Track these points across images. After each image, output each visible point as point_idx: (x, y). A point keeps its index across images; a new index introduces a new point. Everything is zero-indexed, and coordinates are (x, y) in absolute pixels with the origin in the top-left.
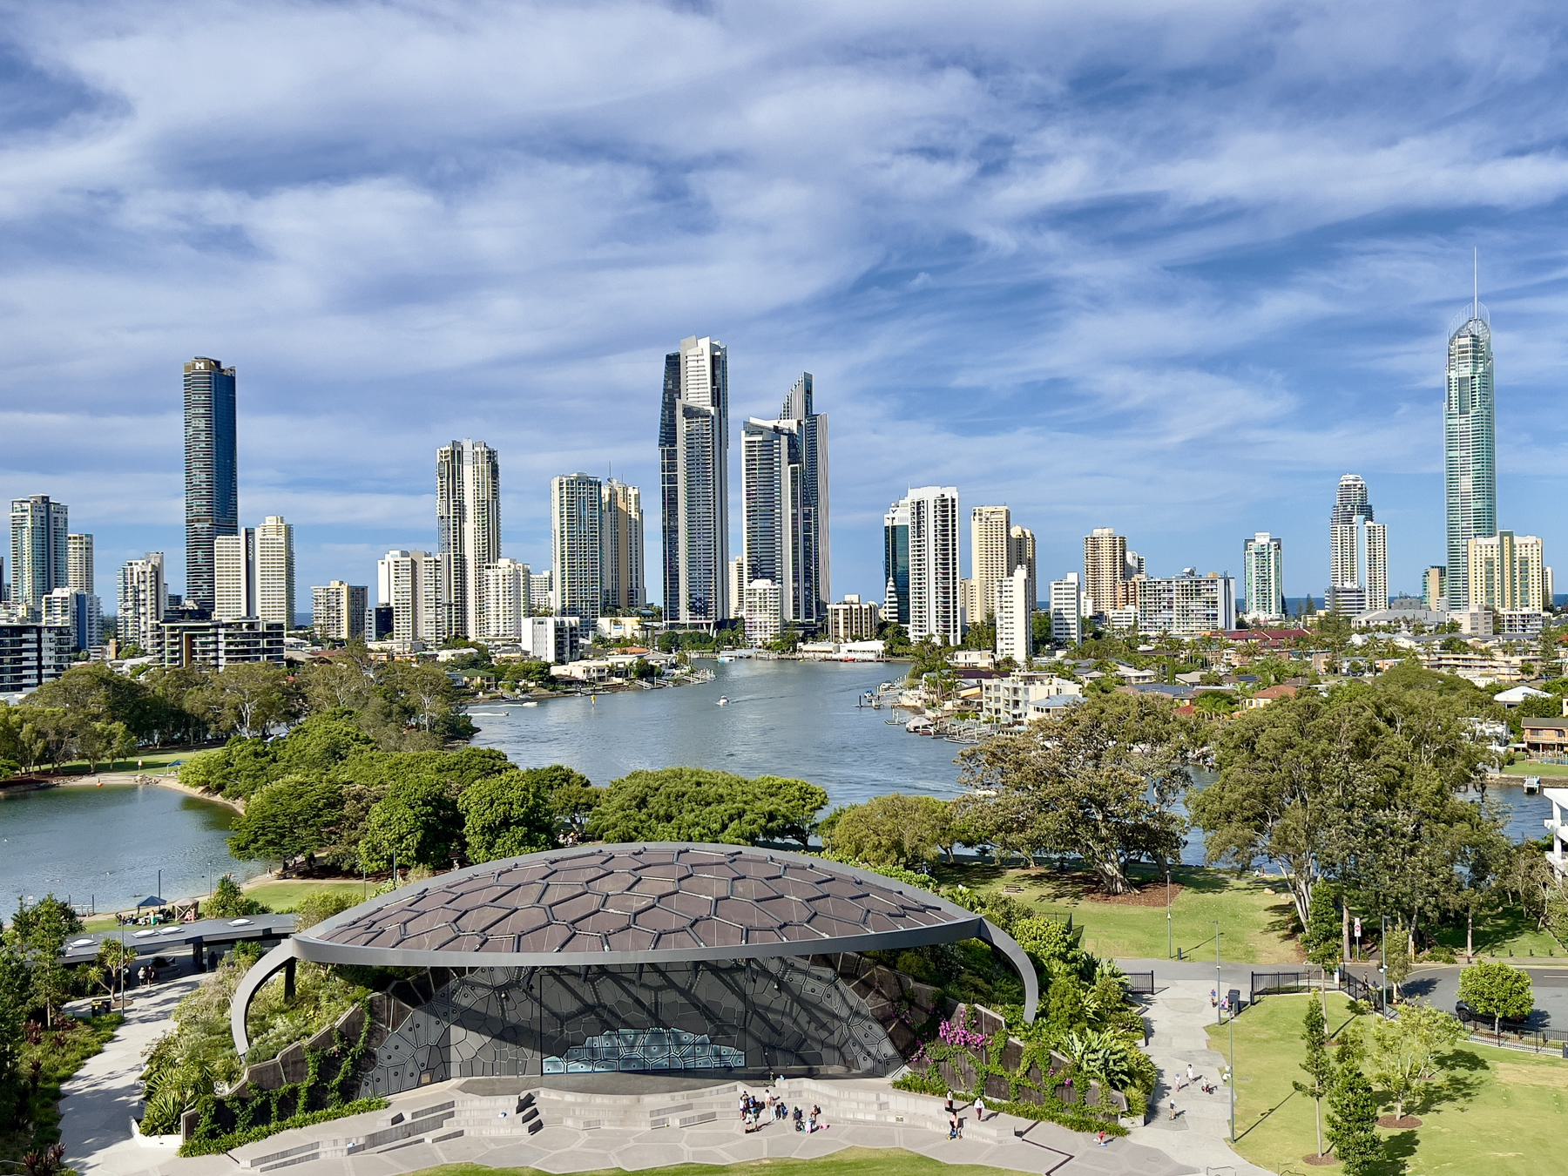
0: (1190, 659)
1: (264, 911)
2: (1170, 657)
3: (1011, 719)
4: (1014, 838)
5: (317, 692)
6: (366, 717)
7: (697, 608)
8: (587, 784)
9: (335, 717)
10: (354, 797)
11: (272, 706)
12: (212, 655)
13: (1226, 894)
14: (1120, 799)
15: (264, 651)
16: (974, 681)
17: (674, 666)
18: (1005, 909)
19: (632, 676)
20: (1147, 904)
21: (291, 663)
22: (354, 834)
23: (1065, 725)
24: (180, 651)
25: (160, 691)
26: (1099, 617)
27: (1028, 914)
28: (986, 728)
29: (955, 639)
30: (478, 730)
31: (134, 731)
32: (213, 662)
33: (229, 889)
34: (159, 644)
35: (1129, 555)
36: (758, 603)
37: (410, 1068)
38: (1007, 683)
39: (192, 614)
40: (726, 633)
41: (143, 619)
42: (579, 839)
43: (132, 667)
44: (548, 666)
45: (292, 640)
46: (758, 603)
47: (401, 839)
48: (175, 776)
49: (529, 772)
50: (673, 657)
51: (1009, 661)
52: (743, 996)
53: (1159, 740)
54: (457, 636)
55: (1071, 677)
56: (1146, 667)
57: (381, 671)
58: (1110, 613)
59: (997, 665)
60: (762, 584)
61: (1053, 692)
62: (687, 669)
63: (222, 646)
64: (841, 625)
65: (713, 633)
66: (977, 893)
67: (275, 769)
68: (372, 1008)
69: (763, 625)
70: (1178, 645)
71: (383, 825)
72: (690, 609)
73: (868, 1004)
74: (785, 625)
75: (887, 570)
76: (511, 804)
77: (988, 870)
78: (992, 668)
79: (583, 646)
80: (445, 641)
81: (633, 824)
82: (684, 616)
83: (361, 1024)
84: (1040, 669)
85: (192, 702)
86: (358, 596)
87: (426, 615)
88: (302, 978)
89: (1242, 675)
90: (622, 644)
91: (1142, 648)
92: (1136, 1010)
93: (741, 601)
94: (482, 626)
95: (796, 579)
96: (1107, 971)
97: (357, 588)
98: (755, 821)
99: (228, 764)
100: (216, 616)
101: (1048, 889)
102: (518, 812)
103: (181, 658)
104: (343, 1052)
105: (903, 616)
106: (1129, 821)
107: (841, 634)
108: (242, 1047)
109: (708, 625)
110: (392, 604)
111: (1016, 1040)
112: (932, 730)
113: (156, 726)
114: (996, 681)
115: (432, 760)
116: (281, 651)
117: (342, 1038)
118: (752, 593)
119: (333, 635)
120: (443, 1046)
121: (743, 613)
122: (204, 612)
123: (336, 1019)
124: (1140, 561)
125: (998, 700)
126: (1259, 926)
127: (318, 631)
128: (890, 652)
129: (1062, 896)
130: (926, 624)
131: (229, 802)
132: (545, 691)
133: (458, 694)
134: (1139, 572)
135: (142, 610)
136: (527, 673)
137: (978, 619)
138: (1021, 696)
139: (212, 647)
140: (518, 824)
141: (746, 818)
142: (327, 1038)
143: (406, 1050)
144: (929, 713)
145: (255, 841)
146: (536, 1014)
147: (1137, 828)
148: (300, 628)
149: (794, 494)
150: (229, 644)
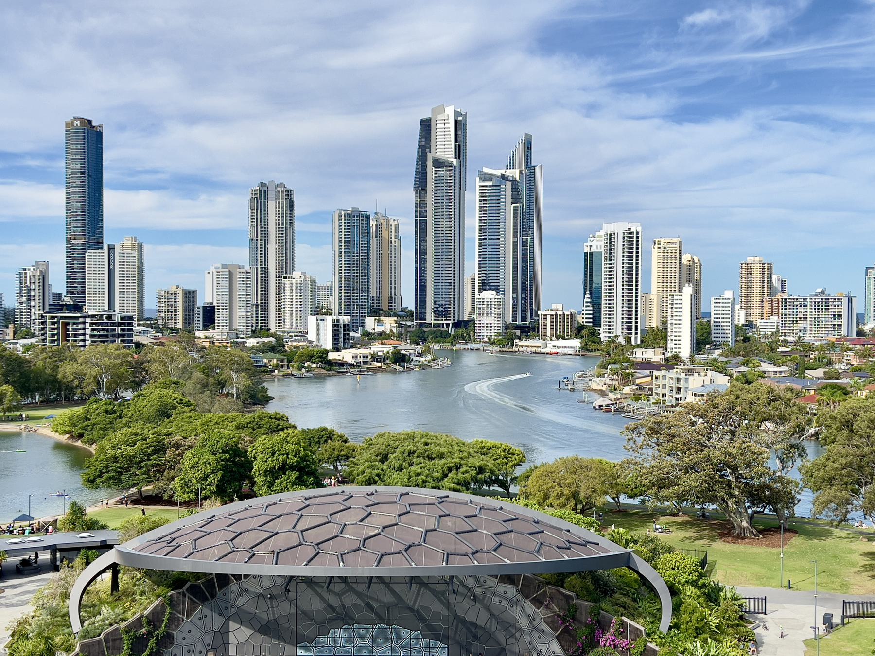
0: (819, 359)
1: (103, 527)
2: (802, 358)
3: (674, 402)
4: (664, 492)
5: (155, 368)
6: (189, 386)
7: (442, 311)
8: (346, 441)
9: (166, 386)
10: (174, 446)
11: (121, 376)
12: (81, 337)
13: (830, 541)
14: (749, 465)
15: (119, 336)
16: (648, 372)
17: (420, 355)
18: (652, 546)
19: (388, 361)
20: (767, 546)
21: (139, 345)
22: (172, 473)
23: (721, 413)
24: (58, 334)
25: (40, 364)
26: (750, 325)
27: (670, 550)
28: (654, 408)
29: (636, 339)
30: (272, 398)
31: (21, 393)
32: (81, 343)
33: (77, 511)
34: (43, 329)
35: (774, 278)
36: (489, 310)
37: (199, 647)
38: (673, 374)
39: (69, 308)
40: (460, 331)
41: (33, 310)
42: (339, 482)
43: (24, 346)
44: (327, 352)
45: (141, 328)
46: (489, 310)
47: (205, 478)
48: (48, 426)
49: (303, 431)
50: (419, 349)
51: (676, 357)
52: (448, 606)
53: (783, 419)
54: (261, 329)
55: (723, 371)
56: (783, 363)
57: (202, 353)
58: (758, 322)
59: (667, 360)
60: (489, 295)
61: (708, 382)
62: (429, 357)
63: (88, 331)
64: (548, 327)
65: (451, 331)
66: (633, 533)
67: (119, 423)
68: (171, 602)
69: (489, 324)
70: (808, 348)
71: (193, 467)
72: (434, 312)
73: (541, 614)
74: (507, 326)
75: (585, 286)
76: (288, 454)
77: (647, 516)
78: (662, 363)
79: (353, 338)
80: (253, 332)
81: (376, 472)
82: (430, 318)
83: (163, 613)
84: (699, 363)
85: (67, 371)
86: (190, 296)
87: (240, 313)
88: (124, 580)
89: (857, 371)
90: (382, 337)
91: (781, 349)
92: (750, 626)
93: (473, 309)
94: (280, 321)
95: (515, 291)
96: (729, 595)
97: (189, 291)
98: (467, 472)
99: (86, 419)
100: (86, 309)
101: (690, 533)
102: (293, 460)
103: (58, 340)
104: (150, 634)
105: (596, 321)
106: (756, 482)
107: (548, 334)
108: (76, 627)
109: (448, 325)
110: (215, 304)
111: (653, 645)
112: (613, 408)
113: (37, 389)
114: (663, 372)
115: (233, 420)
116: (131, 336)
117: (149, 623)
118: (481, 301)
119: (171, 325)
120: (224, 633)
121: (474, 316)
122: (78, 308)
123: (146, 609)
124: (783, 283)
125: (664, 386)
126: (854, 565)
127: (160, 322)
128: (585, 348)
129: (701, 538)
130: (614, 328)
131: (87, 446)
132: (323, 371)
133: (258, 372)
134: (783, 291)
135: (32, 303)
136: (310, 357)
137: (654, 325)
138: (682, 384)
139: (81, 332)
140: (292, 468)
141: (462, 470)
142: (138, 623)
143: (197, 633)
144: (612, 396)
145: (100, 476)
146: (293, 611)
147: (764, 487)
148: (148, 319)
149: (515, 226)
150: (93, 330)
